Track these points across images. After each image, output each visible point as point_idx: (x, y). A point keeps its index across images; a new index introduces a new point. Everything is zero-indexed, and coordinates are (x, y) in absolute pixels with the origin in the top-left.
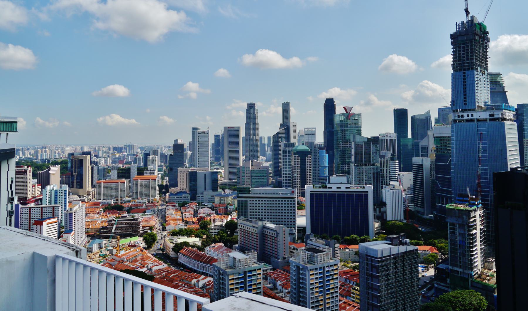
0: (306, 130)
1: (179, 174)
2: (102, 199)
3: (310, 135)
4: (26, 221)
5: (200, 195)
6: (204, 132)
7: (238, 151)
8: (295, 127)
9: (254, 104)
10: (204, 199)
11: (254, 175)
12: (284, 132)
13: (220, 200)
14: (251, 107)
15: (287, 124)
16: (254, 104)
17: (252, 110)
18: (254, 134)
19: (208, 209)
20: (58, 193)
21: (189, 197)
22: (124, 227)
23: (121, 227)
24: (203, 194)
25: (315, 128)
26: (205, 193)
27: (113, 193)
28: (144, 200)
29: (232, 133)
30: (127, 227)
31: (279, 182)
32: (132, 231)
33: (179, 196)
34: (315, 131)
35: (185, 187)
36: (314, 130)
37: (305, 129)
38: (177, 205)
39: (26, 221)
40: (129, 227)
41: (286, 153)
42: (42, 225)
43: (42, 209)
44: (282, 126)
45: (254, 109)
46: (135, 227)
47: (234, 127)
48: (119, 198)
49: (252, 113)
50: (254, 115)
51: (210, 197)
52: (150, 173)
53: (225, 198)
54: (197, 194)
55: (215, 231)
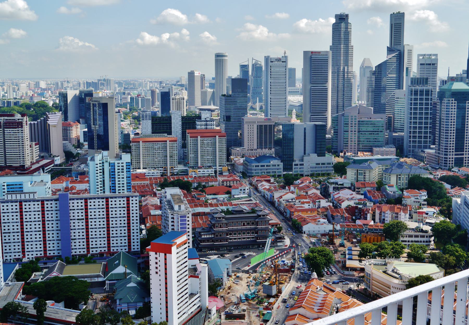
0: (421, 57)
1: (246, 126)
2: (142, 167)
3: (429, 65)
4: (81, 224)
5: (296, 163)
6: (279, 60)
7: (326, 90)
8: (410, 52)
9: (347, 16)
10: (305, 170)
11: (364, 129)
12: (395, 60)
13: (357, 174)
14: (342, 19)
15: (398, 47)
16: (347, 16)
17: (343, 25)
18: (347, 62)
19: (350, 192)
20: (116, 168)
21: (281, 165)
22: (242, 230)
23: (237, 230)
24: (302, 160)
25: (436, 55)
26: (305, 158)
27: (159, 159)
28: (210, 170)
29: (315, 62)
30: (246, 230)
31: (394, 139)
32: (257, 238)
33: (265, 164)
34: (437, 60)
35: (255, 147)
36: (433, 57)
37: (419, 55)
38: (272, 180)
39: (81, 224)
40: (250, 230)
41: (416, 94)
42: (170, 253)
43: (107, 202)
44: (390, 50)
45: (347, 24)
46: (262, 230)
47: (319, 52)
48: (169, 167)
49: (343, 30)
50: (347, 34)
51: (315, 165)
52: (206, 125)
53: (367, 172)
54: (293, 161)
55: (410, 239)
